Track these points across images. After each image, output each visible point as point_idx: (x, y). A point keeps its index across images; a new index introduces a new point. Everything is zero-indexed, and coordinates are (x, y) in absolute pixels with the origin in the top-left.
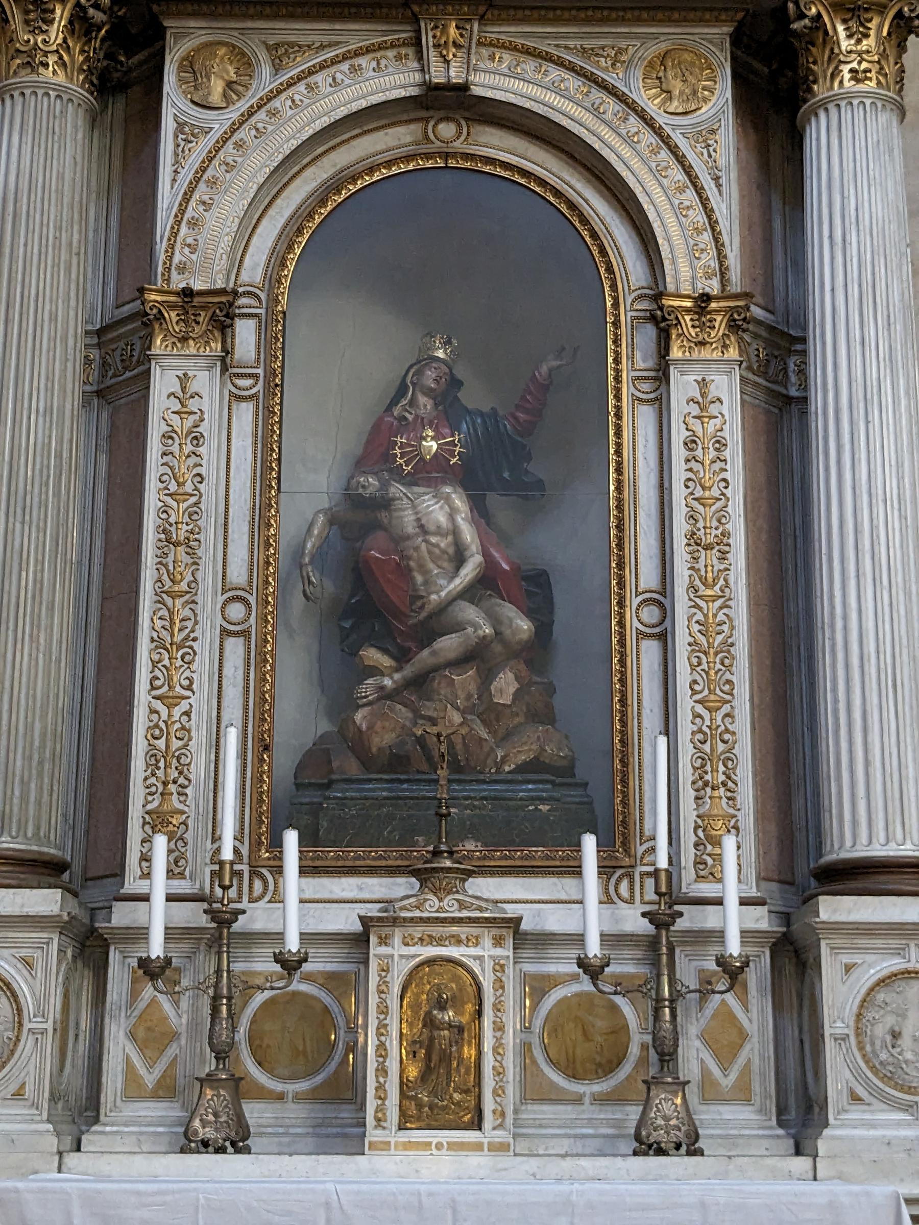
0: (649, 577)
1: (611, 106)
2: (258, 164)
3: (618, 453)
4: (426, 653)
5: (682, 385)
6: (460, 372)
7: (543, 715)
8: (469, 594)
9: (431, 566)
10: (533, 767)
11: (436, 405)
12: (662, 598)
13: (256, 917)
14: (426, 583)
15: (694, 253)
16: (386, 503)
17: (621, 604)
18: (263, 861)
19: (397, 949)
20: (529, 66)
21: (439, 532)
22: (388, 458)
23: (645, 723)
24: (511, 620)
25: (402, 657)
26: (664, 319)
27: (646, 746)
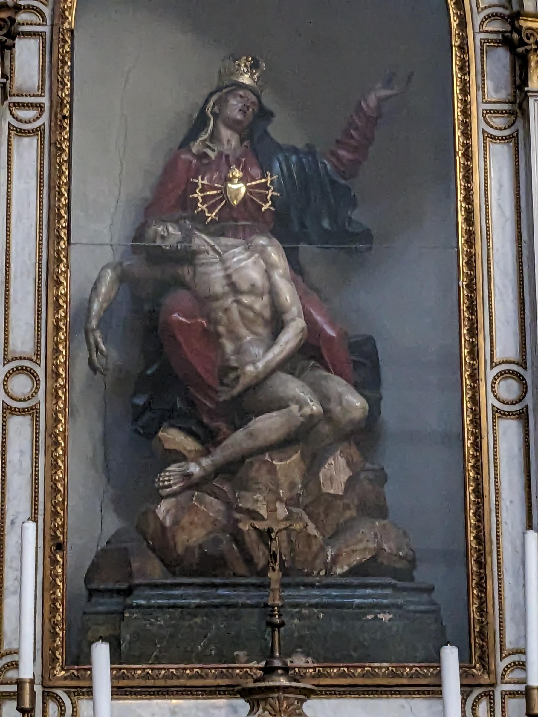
3: (468, 199)
4: (240, 434)
6: (268, 102)
8: (289, 365)
9: (243, 331)
11: (242, 141)
14: (238, 351)
16: (188, 257)
17: (474, 377)
21: (253, 290)
22: (186, 203)
23: (504, 515)
24: (340, 396)
26: (522, 43)
27: (506, 544)
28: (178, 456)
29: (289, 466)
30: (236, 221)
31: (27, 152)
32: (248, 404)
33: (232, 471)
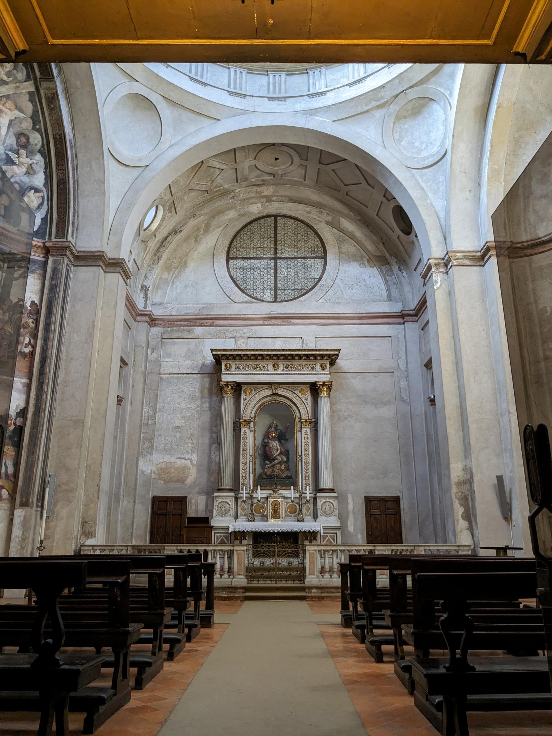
0: (300, 454)
1: (295, 395)
2: (253, 403)
5: (304, 431)
8: (279, 455)
10: (286, 477)
13: (255, 495)
15: (305, 414)
18: (256, 489)
19: (271, 499)
20: (285, 390)
22: (269, 437)
25: (271, 462)
28: (268, 464)
29: (278, 466)
30: (274, 438)
31: (252, 433)
32: (275, 459)
33: (273, 466)
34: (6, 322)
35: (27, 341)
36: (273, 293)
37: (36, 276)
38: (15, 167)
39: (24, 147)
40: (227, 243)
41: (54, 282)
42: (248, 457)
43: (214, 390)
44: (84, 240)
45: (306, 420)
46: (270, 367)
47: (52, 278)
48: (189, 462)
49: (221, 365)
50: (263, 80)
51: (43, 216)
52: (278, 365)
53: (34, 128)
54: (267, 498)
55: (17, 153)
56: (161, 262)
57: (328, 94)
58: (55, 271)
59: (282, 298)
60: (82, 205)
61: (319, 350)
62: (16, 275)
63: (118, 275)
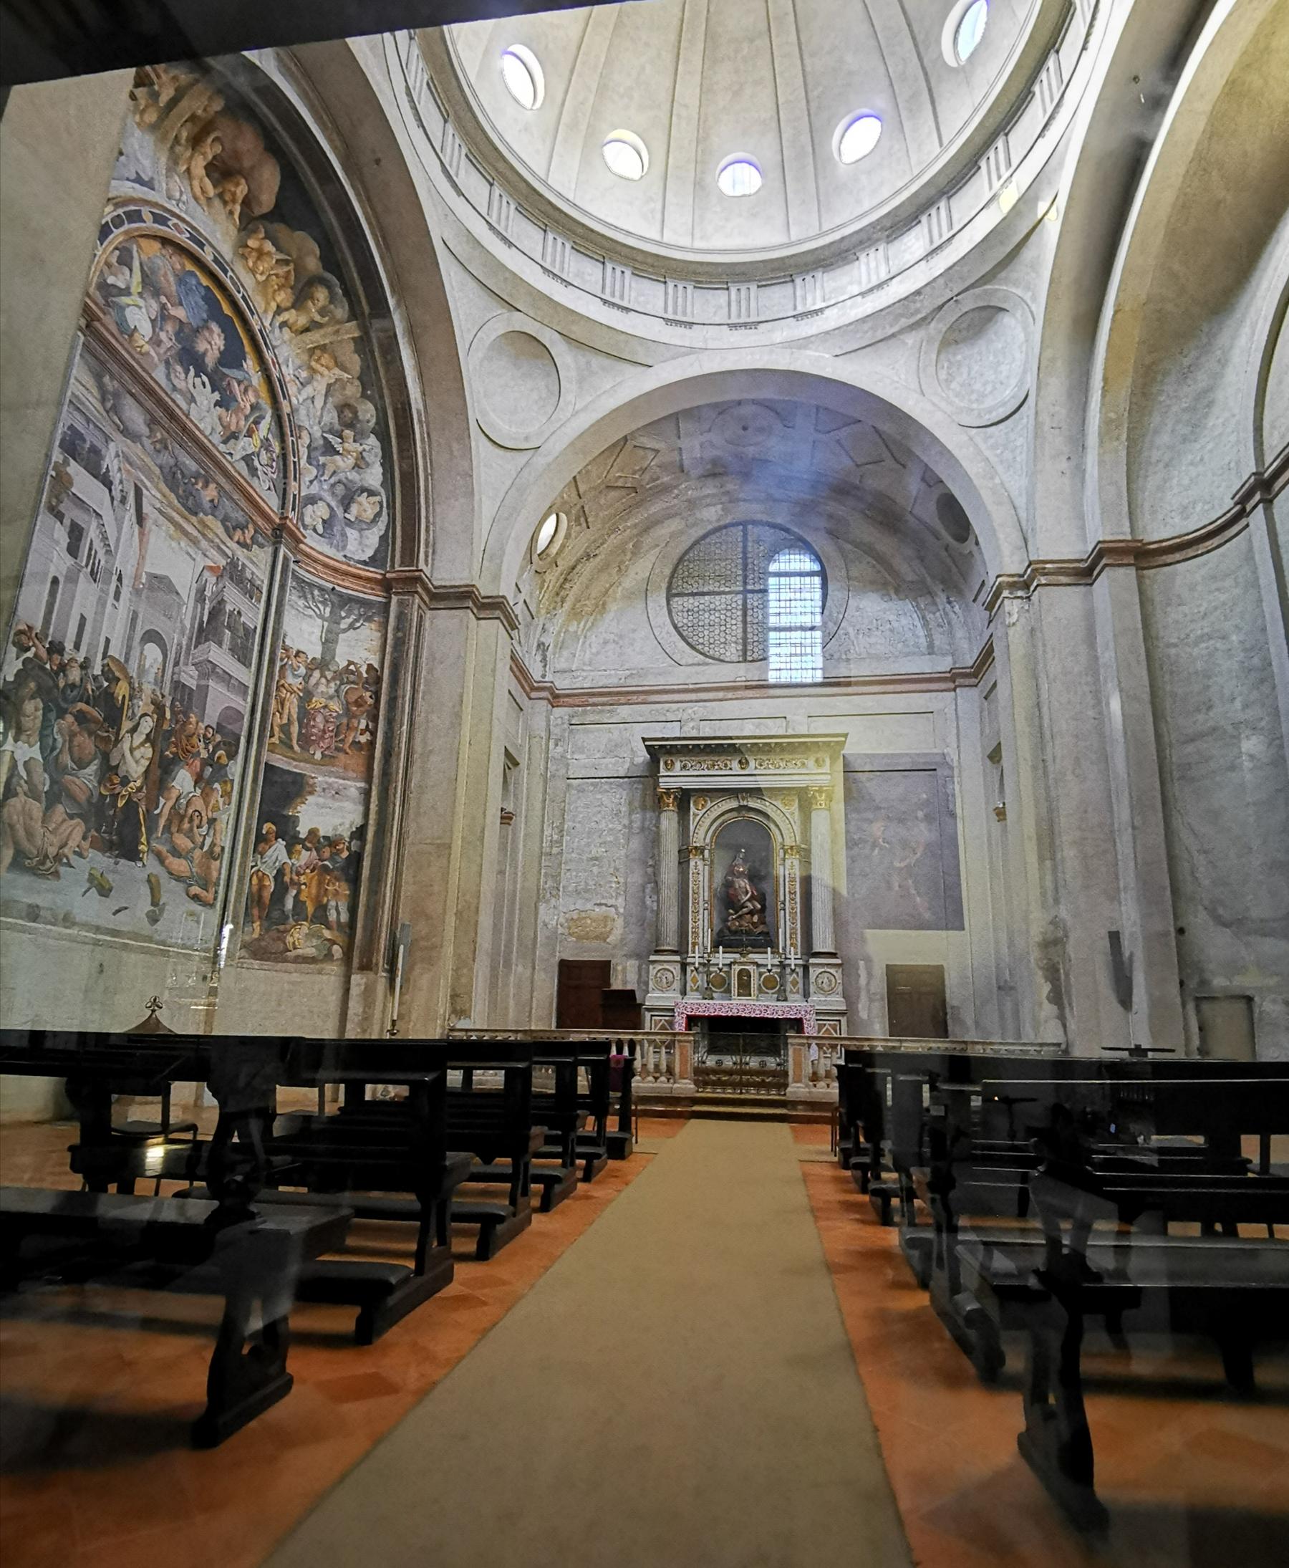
2: (708, 822)
5: (788, 863)
7: (764, 923)
12: (784, 903)
16: (733, 882)
30: (741, 875)
32: (743, 907)
34: (331, 698)
35: (363, 725)
36: (740, 647)
37: (373, 626)
38: (337, 457)
39: (351, 426)
40: (668, 571)
41: (400, 634)
42: (701, 903)
43: (649, 802)
44: (445, 569)
45: (792, 848)
46: (735, 765)
47: (397, 629)
48: (613, 909)
49: (659, 762)
50: (722, 297)
51: (382, 533)
52: (747, 762)
53: (364, 395)
54: (730, 965)
55: (341, 437)
56: (567, 606)
57: (827, 312)
58: (401, 617)
59: (756, 656)
60: (441, 517)
61: (814, 736)
62: (343, 625)
63: (497, 621)
